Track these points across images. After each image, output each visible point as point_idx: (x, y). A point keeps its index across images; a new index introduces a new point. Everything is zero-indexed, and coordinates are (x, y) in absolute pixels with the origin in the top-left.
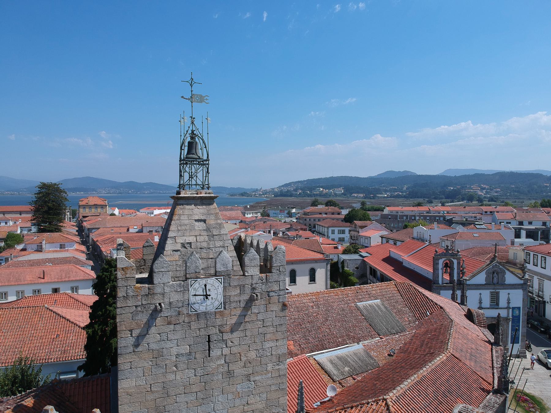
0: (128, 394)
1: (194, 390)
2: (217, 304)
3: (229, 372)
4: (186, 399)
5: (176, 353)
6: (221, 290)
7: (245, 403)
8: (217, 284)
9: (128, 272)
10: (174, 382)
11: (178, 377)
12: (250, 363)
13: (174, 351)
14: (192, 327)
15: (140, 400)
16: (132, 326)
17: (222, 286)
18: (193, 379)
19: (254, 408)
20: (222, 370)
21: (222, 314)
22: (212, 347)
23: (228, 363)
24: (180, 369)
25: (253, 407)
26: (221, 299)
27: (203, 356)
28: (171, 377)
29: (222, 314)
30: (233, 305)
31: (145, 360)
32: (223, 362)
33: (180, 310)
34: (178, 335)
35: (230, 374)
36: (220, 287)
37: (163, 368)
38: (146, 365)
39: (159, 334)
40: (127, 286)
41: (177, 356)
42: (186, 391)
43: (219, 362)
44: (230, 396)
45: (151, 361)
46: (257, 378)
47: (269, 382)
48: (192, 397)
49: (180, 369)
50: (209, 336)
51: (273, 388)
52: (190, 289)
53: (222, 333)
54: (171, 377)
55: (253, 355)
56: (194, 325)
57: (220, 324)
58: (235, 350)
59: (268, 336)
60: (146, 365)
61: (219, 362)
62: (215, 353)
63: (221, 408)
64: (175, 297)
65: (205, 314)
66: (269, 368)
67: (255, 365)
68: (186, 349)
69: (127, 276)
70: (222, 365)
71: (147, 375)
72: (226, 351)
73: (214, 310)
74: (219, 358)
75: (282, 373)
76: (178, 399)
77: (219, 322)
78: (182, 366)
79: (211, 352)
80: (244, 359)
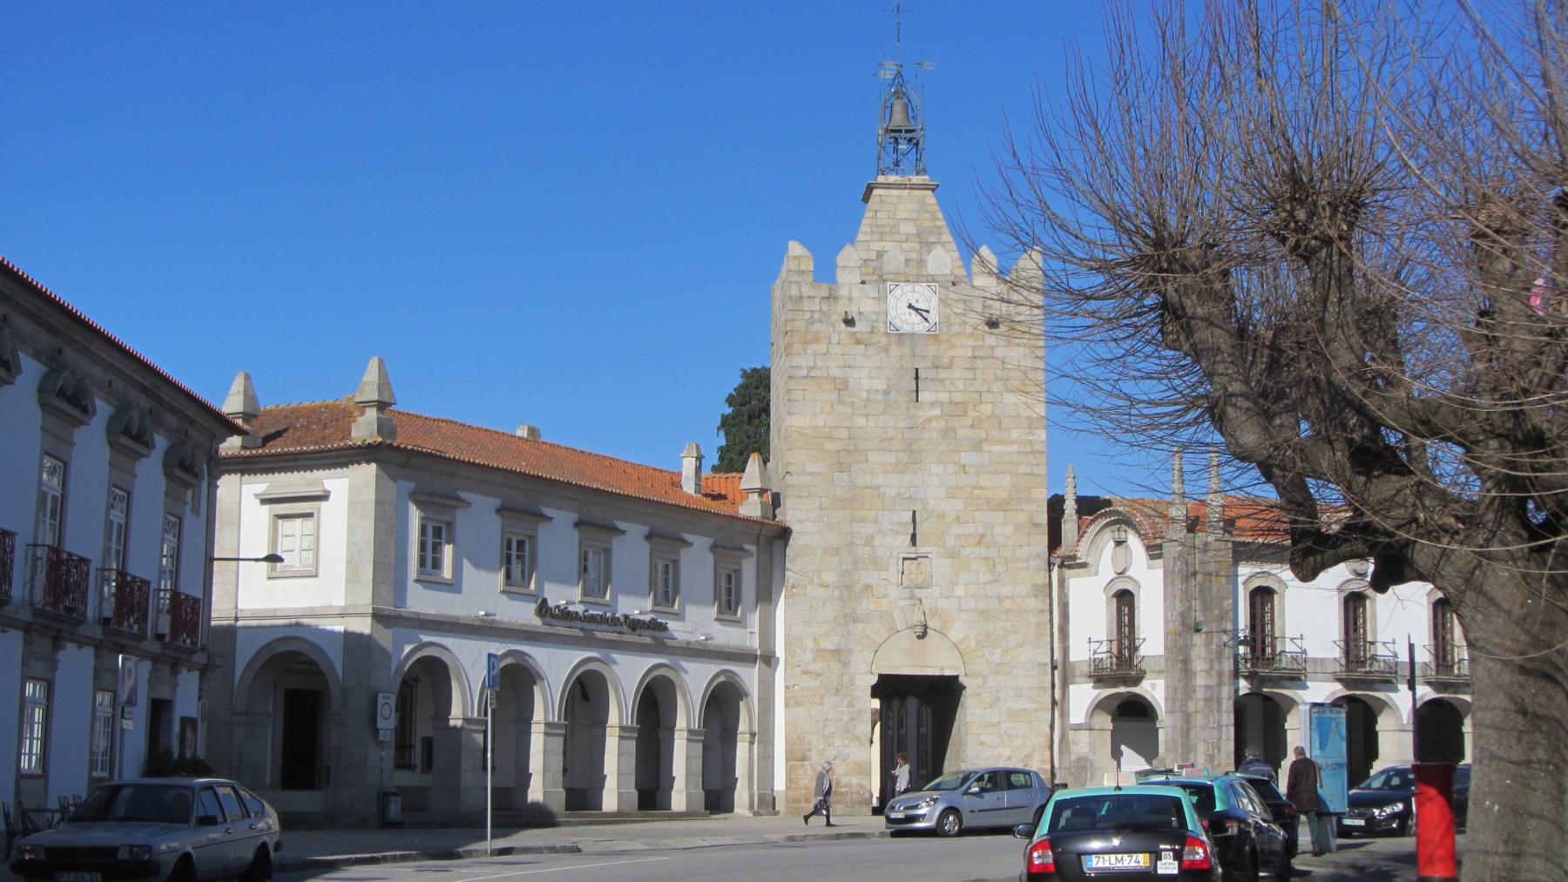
0: (801, 434)
8: (928, 293)
11: (871, 423)
13: (866, 384)
21: (936, 338)
28: (861, 421)
29: (936, 338)
30: (955, 329)
41: (869, 392)
48: (891, 458)
51: (1023, 469)
58: (958, 397)
65: (913, 335)
66: (1015, 434)
68: (880, 384)
70: (937, 418)
72: (944, 397)
74: (933, 405)
80: (972, 413)
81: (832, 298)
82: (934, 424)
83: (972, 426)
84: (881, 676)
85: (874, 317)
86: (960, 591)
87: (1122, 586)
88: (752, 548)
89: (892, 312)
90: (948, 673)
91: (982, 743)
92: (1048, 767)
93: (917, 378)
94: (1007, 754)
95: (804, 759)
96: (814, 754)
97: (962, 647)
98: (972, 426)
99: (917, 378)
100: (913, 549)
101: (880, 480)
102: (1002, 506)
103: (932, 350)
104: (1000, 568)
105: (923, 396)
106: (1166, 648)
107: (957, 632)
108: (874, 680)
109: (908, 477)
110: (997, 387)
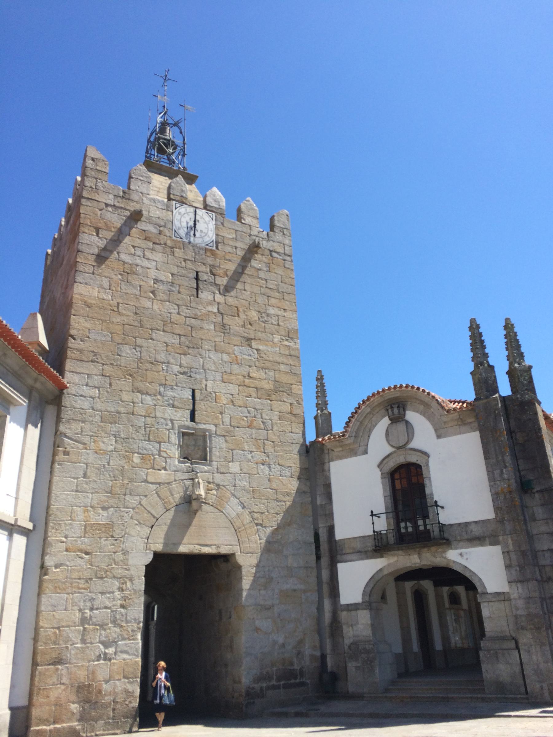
0: (86, 303)
1: (177, 331)
2: (207, 239)
3: (224, 325)
4: (166, 340)
5: (154, 277)
6: (212, 225)
7: (245, 374)
8: (207, 218)
9: (100, 164)
10: (150, 311)
12: (250, 324)
13: (153, 273)
14: (176, 255)
15: (103, 318)
16: (100, 225)
17: (214, 222)
18: (175, 317)
19: (258, 386)
20: (214, 320)
22: (201, 286)
23: (222, 314)
24: (158, 298)
25: (258, 384)
26: (211, 236)
27: (190, 293)
28: (148, 304)
29: (213, 253)
31: (113, 270)
32: (216, 310)
33: (161, 229)
34: (158, 257)
35: (224, 328)
36: (210, 223)
37: (136, 289)
38: (114, 277)
39: (134, 247)
40: (96, 179)
42: (165, 329)
43: (210, 308)
44: (226, 357)
45: (121, 274)
46: (261, 347)
47: (277, 359)
49: (158, 298)
50: (197, 272)
52: (174, 211)
53: (214, 275)
54: (148, 304)
55: (254, 315)
56: (178, 252)
57: (211, 263)
59: (273, 301)
60: (114, 277)
61: (210, 308)
62: (205, 295)
63: (214, 369)
64: (156, 213)
67: (257, 329)
69: (98, 168)
70: (214, 313)
71: (114, 289)
73: (203, 245)
75: (292, 353)
76: (154, 334)
77: (210, 261)
78: (161, 296)
79: (200, 292)
80: (242, 316)
81: (126, 196)
82: (212, 318)
83: (244, 326)
84: (157, 555)
85: (162, 223)
86: (234, 467)
87: (401, 459)
88: (23, 402)
89: (177, 223)
90: (224, 550)
91: (257, 630)
92: (318, 653)
93: (197, 278)
94: (281, 640)
95: (58, 661)
96: (71, 654)
97: (238, 524)
98: (244, 326)
99: (197, 278)
101: (162, 357)
102: (269, 396)
103: (210, 261)
104: (269, 448)
105: (201, 295)
106: (497, 509)
107: (233, 508)
108: (149, 558)
109: (185, 360)
110: (261, 300)
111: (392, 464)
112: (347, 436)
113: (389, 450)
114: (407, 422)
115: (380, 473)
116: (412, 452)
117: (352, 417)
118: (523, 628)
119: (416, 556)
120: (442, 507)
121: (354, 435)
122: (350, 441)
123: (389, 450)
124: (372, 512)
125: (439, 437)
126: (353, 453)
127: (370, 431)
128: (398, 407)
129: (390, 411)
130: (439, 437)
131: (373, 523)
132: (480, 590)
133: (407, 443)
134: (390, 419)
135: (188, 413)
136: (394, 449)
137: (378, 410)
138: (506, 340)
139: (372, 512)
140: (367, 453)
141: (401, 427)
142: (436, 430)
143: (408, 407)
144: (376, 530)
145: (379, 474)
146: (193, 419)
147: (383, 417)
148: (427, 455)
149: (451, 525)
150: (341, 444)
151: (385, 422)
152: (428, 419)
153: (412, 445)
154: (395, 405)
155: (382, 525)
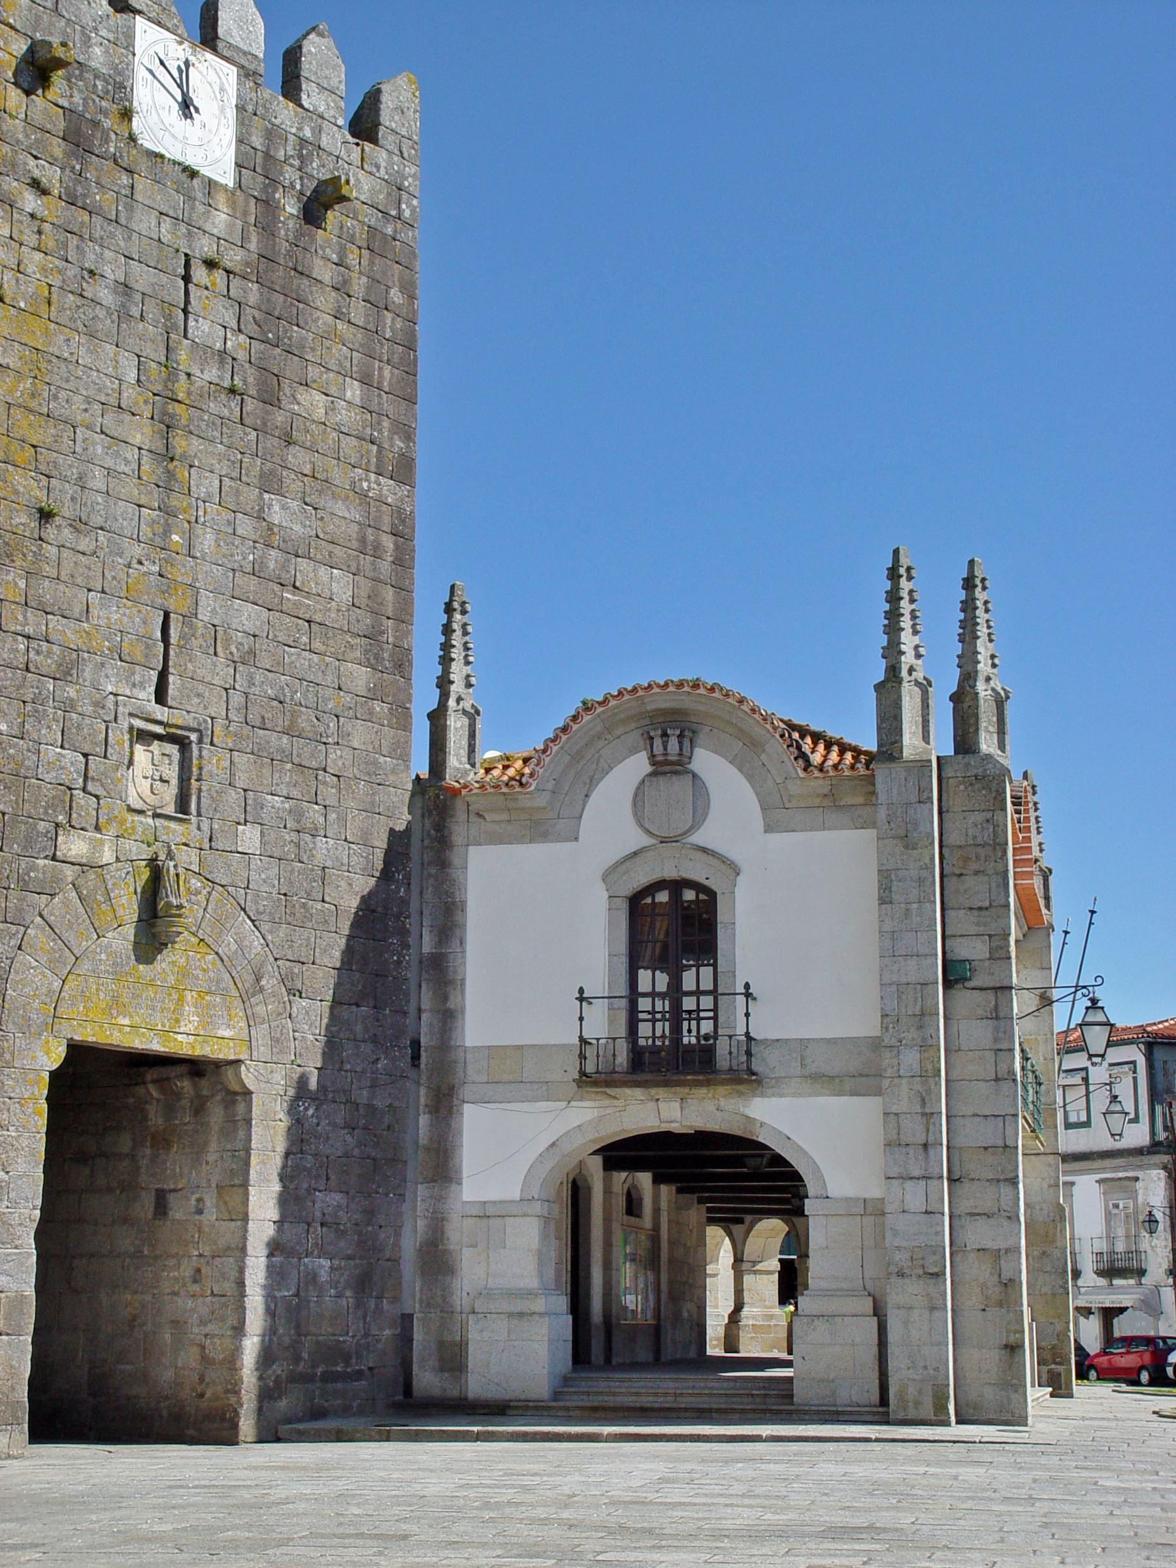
100: (160, 713)
111: (642, 877)
112: (532, 788)
113: (636, 839)
114: (694, 776)
115: (606, 895)
116: (699, 855)
117: (554, 740)
118: (901, 1274)
119: (677, 1105)
120: (755, 999)
121: (550, 785)
122: (542, 801)
123: (636, 839)
124: (581, 991)
125: (768, 829)
126: (538, 829)
127: (592, 783)
128: (681, 736)
129: (658, 743)
130: (768, 829)
131: (581, 1019)
132: (812, 1188)
133: (686, 833)
134: (653, 764)
135: (154, 675)
136: (647, 841)
137: (620, 730)
138: (962, 616)
139: (581, 991)
140: (576, 839)
141: (679, 787)
142: (763, 809)
143: (702, 738)
144: (585, 1036)
145: (601, 895)
146: (161, 696)
147: (634, 751)
148: (735, 870)
149: (764, 1041)
150: (511, 805)
151: (638, 765)
152: (750, 778)
153: (697, 838)
154: (669, 728)
155: (601, 1023)
